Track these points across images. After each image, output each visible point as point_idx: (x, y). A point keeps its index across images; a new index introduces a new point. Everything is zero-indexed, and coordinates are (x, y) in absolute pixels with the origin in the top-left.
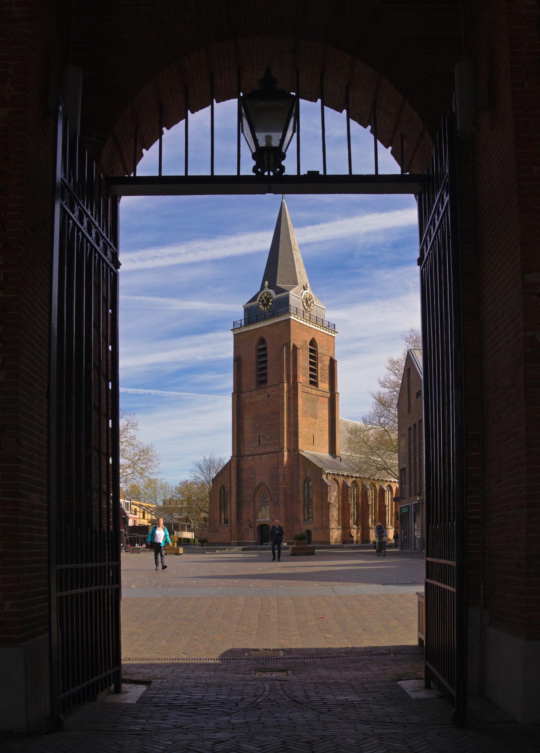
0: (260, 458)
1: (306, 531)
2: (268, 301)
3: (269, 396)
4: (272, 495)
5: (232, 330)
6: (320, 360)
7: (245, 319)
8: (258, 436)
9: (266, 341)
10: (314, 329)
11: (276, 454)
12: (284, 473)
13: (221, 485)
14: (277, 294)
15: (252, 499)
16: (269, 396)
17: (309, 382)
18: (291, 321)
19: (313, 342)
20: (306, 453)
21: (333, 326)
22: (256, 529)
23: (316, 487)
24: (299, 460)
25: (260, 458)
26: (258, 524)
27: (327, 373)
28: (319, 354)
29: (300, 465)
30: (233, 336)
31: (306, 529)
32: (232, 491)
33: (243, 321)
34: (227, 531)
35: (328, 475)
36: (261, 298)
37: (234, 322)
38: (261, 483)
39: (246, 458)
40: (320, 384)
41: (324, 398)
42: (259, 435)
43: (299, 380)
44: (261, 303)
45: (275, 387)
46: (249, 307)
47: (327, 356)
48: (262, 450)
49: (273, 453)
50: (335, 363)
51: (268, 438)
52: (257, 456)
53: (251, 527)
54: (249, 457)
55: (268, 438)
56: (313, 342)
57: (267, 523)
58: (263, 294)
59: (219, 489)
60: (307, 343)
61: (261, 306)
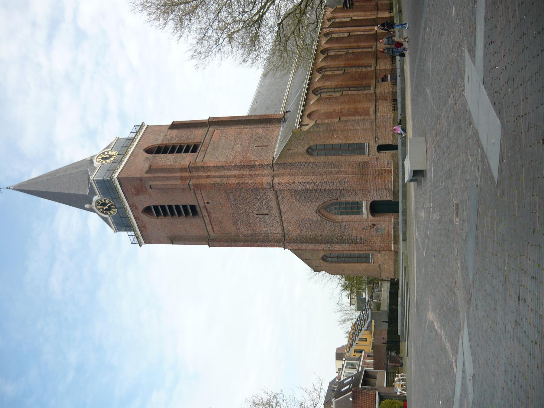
0: (285, 213)
1: (379, 152)
2: (104, 204)
3: (208, 203)
4: (331, 199)
5: (140, 246)
6: (171, 141)
7: (126, 231)
8: (258, 216)
9: (147, 206)
10: (135, 149)
11: (278, 194)
12: (300, 183)
13: (322, 261)
14: (96, 195)
15: (337, 224)
16: (208, 203)
17: (192, 154)
18: (119, 177)
19: (149, 151)
20: (277, 154)
21: (136, 127)
22: (376, 219)
23: (318, 139)
24: (284, 164)
25: (285, 213)
26: (370, 216)
27: (186, 133)
28: (163, 143)
29: (290, 162)
30: (147, 245)
31: (376, 151)
32: (327, 249)
33: (130, 233)
34: (379, 254)
35: (304, 123)
37: (132, 243)
38: (316, 212)
39: (286, 231)
40: (197, 141)
41: (214, 135)
42: (257, 214)
43: (186, 165)
44: (108, 212)
45: (197, 196)
46: (115, 226)
47: (166, 134)
48: (275, 212)
49: (277, 197)
50: (175, 123)
51: (259, 203)
52: (283, 219)
53: (374, 225)
54: (285, 227)
56: (149, 151)
57: (369, 205)
58: (99, 209)
59: (326, 263)
60: (148, 158)
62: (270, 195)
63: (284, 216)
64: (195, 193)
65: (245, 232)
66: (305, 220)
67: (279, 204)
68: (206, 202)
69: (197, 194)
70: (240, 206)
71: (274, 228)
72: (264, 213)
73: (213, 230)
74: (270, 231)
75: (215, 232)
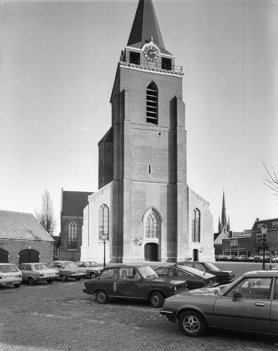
3: (160, 134)
16: (160, 134)
36: (147, 48)
42: (150, 166)
44: (146, 53)
66: (145, 198)
68: (161, 132)
70: (157, 155)
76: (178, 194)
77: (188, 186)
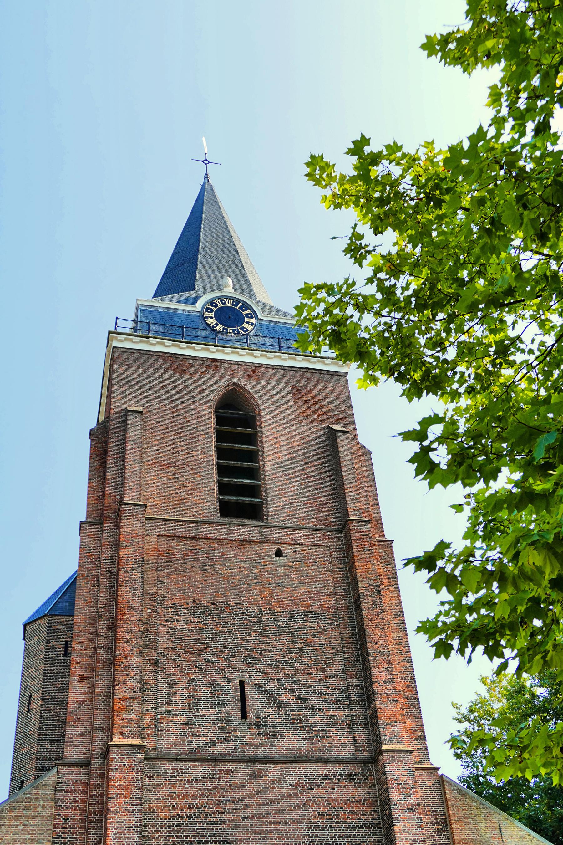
0: (254, 776)
16: (279, 553)
25: (254, 776)
36: (212, 303)
37: (117, 318)
42: (242, 683)
46: (160, 310)
49: (325, 761)
54: (190, 765)
55: (288, 697)
61: (211, 322)
62: (328, 740)
63: (240, 769)
64: (316, 530)
65: (163, 630)
67: (292, 762)
69: (313, 533)
71: (180, 727)
72: (248, 709)
73: (172, 537)
74: (169, 712)
75: (164, 539)
76: (396, 812)
77: (440, 772)
